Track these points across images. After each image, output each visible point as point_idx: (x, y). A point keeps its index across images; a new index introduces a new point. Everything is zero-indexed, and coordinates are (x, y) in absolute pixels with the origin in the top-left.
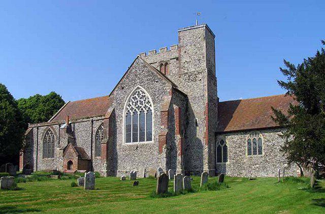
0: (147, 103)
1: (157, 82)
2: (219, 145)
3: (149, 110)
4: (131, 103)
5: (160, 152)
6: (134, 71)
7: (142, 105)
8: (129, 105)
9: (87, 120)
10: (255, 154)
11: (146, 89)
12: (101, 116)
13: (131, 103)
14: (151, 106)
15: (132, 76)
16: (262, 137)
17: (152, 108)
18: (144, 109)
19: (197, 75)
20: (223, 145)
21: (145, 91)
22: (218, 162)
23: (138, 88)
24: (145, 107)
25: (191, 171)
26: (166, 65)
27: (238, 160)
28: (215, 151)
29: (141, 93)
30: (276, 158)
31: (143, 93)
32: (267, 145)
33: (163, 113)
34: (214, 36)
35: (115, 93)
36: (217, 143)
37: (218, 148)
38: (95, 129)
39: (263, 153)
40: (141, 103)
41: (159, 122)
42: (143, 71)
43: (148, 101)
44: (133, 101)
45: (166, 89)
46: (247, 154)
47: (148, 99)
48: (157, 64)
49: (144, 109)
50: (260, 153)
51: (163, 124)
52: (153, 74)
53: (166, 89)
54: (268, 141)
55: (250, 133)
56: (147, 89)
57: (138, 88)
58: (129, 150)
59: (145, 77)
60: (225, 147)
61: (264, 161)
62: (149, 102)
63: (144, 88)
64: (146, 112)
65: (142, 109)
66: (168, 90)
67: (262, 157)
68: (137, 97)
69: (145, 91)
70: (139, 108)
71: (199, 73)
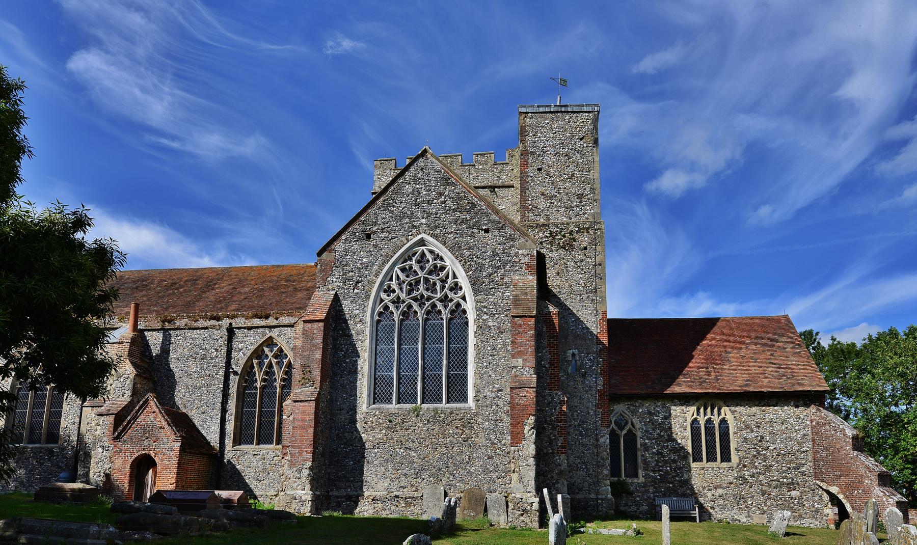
0: (451, 289)
1: (487, 231)
3: (458, 312)
4: (394, 284)
5: (517, 437)
6: (408, 189)
7: (434, 291)
8: (389, 291)
9: (213, 322)
10: (711, 458)
11: (451, 249)
12: (267, 317)
13: (394, 284)
14: (464, 298)
15: (400, 206)
16: (729, 417)
17: (469, 306)
18: (440, 306)
20: (624, 432)
23: (422, 243)
24: (445, 300)
27: (667, 473)
29: (429, 256)
30: (767, 474)
31: (438, 257)
32: (746, 439)
33: (519, 321)
35: (339, 246)
38: (240, 359)
39: (735, 459)
40: (431, 288)
41: (494, 348)
42: (440, 194)
43: (456, 284)
44: (402, 277)
45: (516, 255)
47: (455, 276)
49: (440, 306)
50: (726, 457)
51: (519, 354)
52: (473, 206)
53: (516, 255)
54: (747, 427)
55: (697, 404)
56: (455, 249)
57: (422, 243)
58: (389, 428)
59: (446, 212)
60: (631, 438)
61: (738, 479)
62: (456, 287)
63: (444, 244)
64: (445, 315)
65: (434, 306)
66: (525, 260)
67: (731, 468)
68: (416, 267)
70: (420, 300)
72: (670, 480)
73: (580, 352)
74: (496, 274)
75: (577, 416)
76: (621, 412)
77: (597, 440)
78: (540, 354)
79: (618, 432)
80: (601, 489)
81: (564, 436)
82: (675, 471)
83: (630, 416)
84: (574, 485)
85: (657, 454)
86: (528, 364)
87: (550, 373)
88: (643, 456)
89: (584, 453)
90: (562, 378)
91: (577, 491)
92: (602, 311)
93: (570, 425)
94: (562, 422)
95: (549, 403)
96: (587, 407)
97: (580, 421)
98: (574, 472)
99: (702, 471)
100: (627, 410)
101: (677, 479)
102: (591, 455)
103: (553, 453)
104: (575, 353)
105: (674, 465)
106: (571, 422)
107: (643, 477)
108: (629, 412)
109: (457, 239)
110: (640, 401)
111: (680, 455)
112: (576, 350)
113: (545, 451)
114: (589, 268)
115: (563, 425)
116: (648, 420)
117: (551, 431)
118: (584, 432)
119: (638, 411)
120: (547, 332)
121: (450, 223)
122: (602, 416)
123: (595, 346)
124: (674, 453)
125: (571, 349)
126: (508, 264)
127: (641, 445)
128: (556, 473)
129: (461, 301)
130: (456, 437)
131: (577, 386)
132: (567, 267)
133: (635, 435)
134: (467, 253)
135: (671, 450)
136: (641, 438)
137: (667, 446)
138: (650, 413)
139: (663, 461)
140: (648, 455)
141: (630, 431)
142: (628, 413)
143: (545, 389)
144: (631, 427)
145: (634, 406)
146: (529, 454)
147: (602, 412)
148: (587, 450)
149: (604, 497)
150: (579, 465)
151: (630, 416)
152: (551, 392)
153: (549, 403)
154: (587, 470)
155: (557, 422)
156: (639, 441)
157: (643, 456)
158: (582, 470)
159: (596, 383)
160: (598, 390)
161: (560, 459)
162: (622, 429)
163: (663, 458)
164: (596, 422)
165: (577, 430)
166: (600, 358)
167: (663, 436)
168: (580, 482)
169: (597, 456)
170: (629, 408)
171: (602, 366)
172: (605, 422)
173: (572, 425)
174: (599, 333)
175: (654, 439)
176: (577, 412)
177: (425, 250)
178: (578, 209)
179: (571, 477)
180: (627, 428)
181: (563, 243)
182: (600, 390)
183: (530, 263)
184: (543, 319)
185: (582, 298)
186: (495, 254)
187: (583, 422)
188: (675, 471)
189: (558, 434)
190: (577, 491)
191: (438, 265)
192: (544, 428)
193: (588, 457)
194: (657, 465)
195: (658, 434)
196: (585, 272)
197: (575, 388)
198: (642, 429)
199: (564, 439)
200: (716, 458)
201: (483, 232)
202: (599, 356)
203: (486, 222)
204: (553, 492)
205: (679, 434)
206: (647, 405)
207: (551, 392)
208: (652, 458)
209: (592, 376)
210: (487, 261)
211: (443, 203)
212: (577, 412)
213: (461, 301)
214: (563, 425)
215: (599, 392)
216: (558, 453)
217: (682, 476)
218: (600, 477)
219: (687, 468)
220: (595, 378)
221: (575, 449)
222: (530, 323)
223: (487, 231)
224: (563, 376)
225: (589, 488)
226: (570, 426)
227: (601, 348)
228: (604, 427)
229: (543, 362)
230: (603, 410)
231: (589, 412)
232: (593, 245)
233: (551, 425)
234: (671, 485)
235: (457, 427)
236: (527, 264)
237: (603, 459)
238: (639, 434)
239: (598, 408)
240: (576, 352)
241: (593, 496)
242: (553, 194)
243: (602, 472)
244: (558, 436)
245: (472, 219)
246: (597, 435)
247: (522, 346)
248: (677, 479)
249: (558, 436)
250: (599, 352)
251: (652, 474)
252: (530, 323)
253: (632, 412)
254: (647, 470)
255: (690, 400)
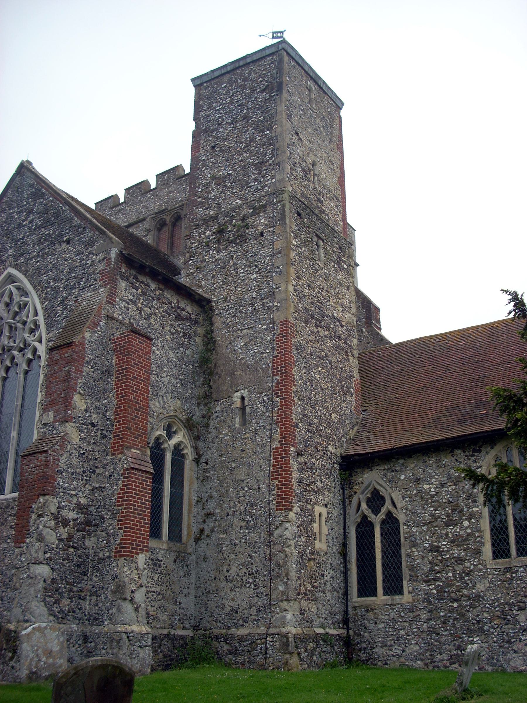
2: (364, 517)
14: (40, 342)
19: (250, 220)
20: (382, 515)
21: (29, 287)
22: (360, 595)
25: (217, 638)
26: (174, 225)
27: (448, 583)
28: (344, 545)
33: (56, 355)
34: (338, 105)
36: (351, 510)
37: (359, 526)
42: (30, 212)
46: (487, 550)
48: (146, 225)
66: (101, 266)
69: (29, 287)
71: (257, 211)
72: (453, 595)
73: (251, 393)
74: (69, 298)
75: (244, 496)
76: (375, 484)
77: (270, 534)
78: (106, 401)
79: (372, 517)
80: (274, 618)
81: (126, 528)
82: (462, 578)
83: (388, 488)
84: (237, 612)
85: (431, 551)
86: (57, 418)
87: (114, 427)
88: (408, 555)
89: (251, 557)
90: (226, 438)
91: (241, 622)
92: (281, 322)
93: (234, 511)
94: (123, 505)
95: (111, 476)
96: (258, 481)
97: (247, 504)
98: (237, 590)
99: (508, 576)
100: (382, 478)
101: (465, 592)
102: (261, 560)
103: (109, 557)
104: (244, 395)
105: (459, 568)
106: (235, 506)
107: (409, 592)
108: (385, 482)
109: (38, 264)
110: (401, 461)
111: (469, 548)
112: (246, 390)
113: (101, 555)
114: (264, 263)
115: (125, 509)
116: (415, 492)
117: (110, 521)
118: (252, 522)
119: (400, 479)
120: (116, 365)
121: (34, 244)
122: (277, 492)
123: (270, 379)
124: (458, 546)
125: (238, 391)
126: (83, 279)
127: (405, 538)
128: (111, 590)
129: (37, 344)
130: (9, 541)
131: (244, 447)
132: (237, 268)
133: (397, 521)
134: (45, 278)
135: (453, 542)
136: (405, 524)
137: (447, 534)
138: (418, 481)
139: (441, 561)
140: (416, 554)
141: (389, 514)
142: (384, 485)
143: (107, 455)
144: (391, 508)
145: (393, 471)
146: (31, 559)
147: (277, 485)
148: (256, 552)
149: (275, 631)
150: (244, 579)
151: (388, 488)
152: (114, 459)
153: (111, 476)
154: (255, 586)
155: (118, 506)
156: (403, 529)
157: (408, 555)
158: (248, 586)
159: (271, 437)
160: (273, 449)
161: (118, 566)
162: (376, 512)
163: (441, 555)
164: (269, 504)
165: (243, 520)
166: (277, 397)
167: (439, 517)
168: (245, 606)
169: (270, 560)
170: (385, 475)
171: (279, 409)
172: (282, 502)
173: (237, 511)
174: (276, 357)
175: (425, 524)
176: (243, 489)
177: (12, 288)
178: (256, 183)
179: (233, 600)
180: (384, 510)
181: (234, 236)
182: (277, 448)
183: (105, 269)
184: (113, 346)
185: (255, 309)
186: (71, 270)
187: (252, 505)
188: (462, 578)
189: (118, 525)
190: (241, 622)
191: (21, 303)
192: (102, 518)
193: (257, 563)
194: (432, 570)
195: (433, 515)
196: (260, 269)
197: (243, 451)
198: (406, 509)
199: (124, 532)
200: (509, 551)
201: (65, 244)
202: (275, 394)
203: (67, 231)
204: (106, 623)
205: (466, 510)
206: (412, 466)
207: (114, 459)
208: (423, 558)
209: (265, 428)
210: (63, 281)
211: (31, 222)
212: (243, 489)
213: (37, 344)
214: (125, 509)
215: (274, 452)
216: (116, 556)
217: (474, 587)
218: (273, 597)
219: (480, 570)
220: (270, 430)
221: (240, 552)
222: (66, 355)
223: (68, 242)
224: (227, 435)
225: (257, 615)
226: (234, 514)
227: (278, 380)
228: (281, 510)
229: (108, 413)
230: (279, 482)
231: (259, 488)
232: (271, 227)
233: (110, 511)
234: (455, 605)
235: (11, 527)
236: (101, 273)
237: (278, 565)
238: (402, 518)
239: (272, 479)
240: (245, 393)
241: (262, 629)
242: (226, 174)
243: (276, 588)
244: (117, 527)
245: (54, 232)
246: (270, 524)
247: (55, 392)
248: (465, 592)
249: (117, 527)
250: (276, 387)
251: (424, 586)
252: (66, 355)
253: (390, 481)
254: (415, 581)
255: (480, 447)
